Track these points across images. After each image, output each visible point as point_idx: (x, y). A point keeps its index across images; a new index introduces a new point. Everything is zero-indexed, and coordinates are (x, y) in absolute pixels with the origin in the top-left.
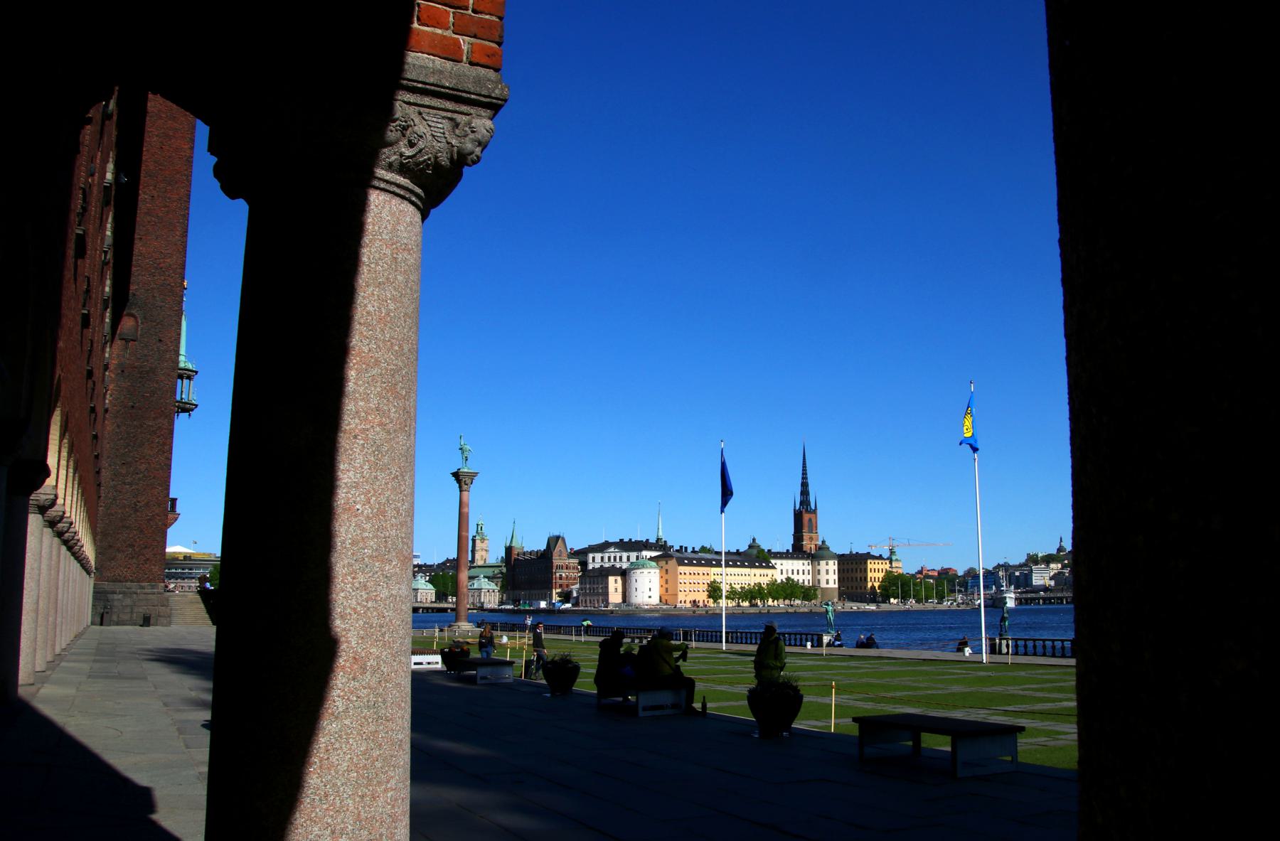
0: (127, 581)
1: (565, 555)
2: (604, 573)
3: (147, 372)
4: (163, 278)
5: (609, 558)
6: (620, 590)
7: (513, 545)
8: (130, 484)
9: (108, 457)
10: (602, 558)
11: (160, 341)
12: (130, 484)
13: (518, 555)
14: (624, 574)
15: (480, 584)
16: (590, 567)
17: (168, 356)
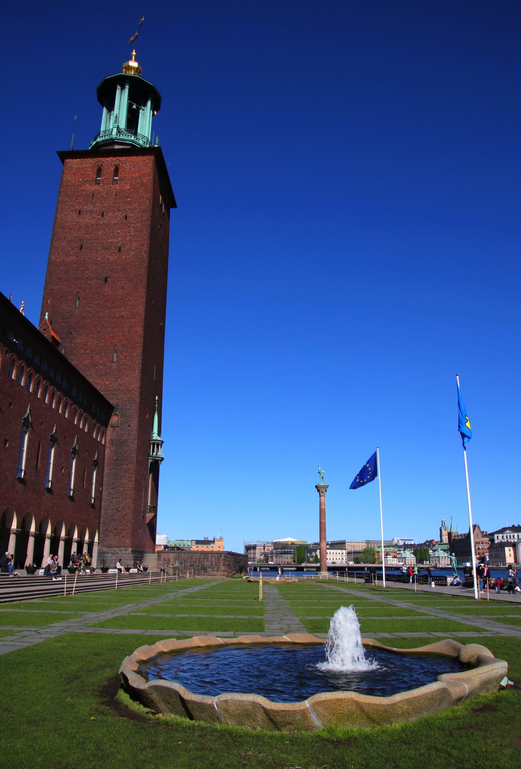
0: (114, 547)
1: (480, 535)
2: (502, 545)
3: (123, 442)
4: (130, 395)
5: (507, 537)
6: (512, 555)
7: (452, 531)
8: (116, 498)
9: (106, 485)
10: (503, 537)
11: (129, 426)
12: (116, 498)
13: (455, 537)
14: (514, 545)
15: (439, 554)
16: (496, 542)
17: (133, 433)
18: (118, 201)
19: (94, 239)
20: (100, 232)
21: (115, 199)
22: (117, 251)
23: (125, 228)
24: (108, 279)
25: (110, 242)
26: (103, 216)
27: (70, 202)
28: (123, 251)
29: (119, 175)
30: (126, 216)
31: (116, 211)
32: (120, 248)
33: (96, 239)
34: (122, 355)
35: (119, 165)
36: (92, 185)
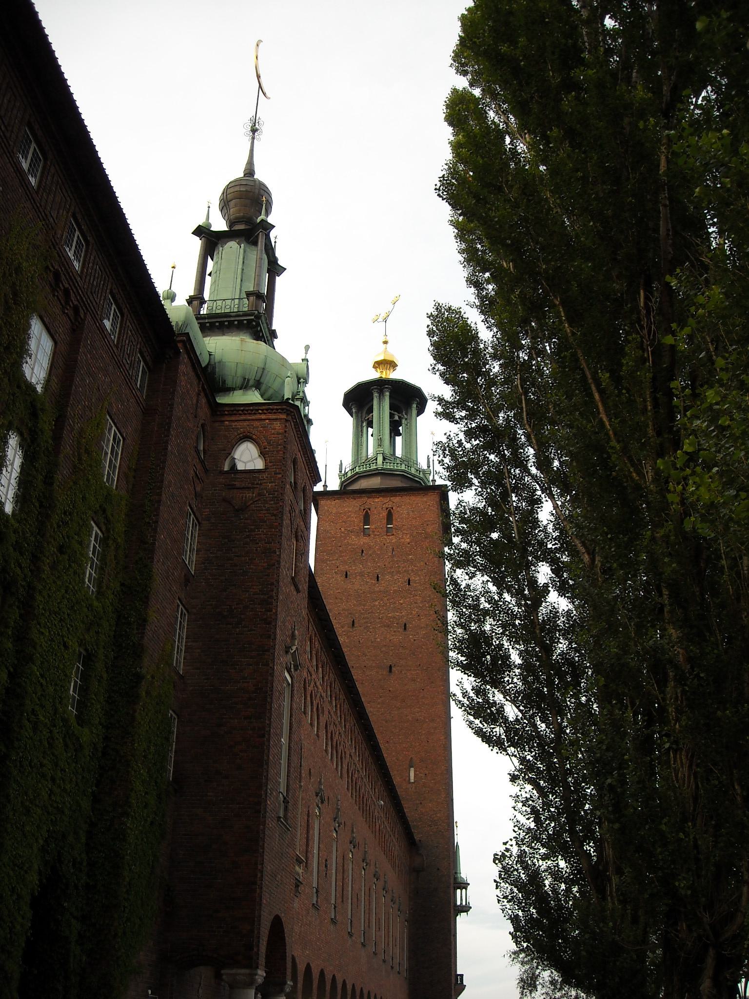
18: (396, 559)
19: (369, 613)
20: (377, 603)
21: (393, 556)
22: (401, 630)
23: (410, 598)
24: (393, 669)
25: (391, 617)
26: (378, 580)
27: (332, 561)
28: (410, 630)
29: (394, 522)
30: (409, 580)
31: (394, 573)
32: (405, 625)
33: (372, 612)
34: (421, 773)
35: (392, 508)
36: (358, 536)
